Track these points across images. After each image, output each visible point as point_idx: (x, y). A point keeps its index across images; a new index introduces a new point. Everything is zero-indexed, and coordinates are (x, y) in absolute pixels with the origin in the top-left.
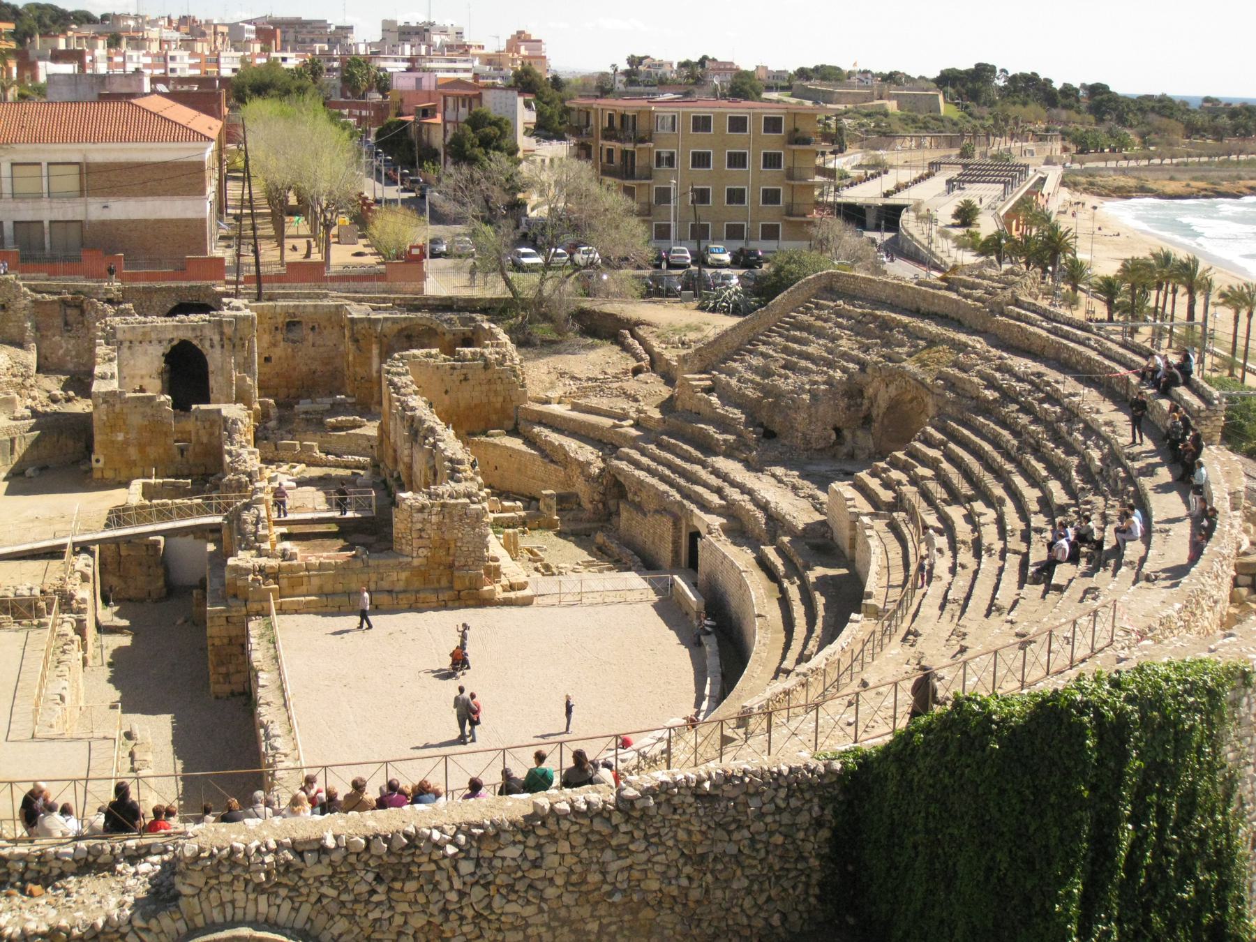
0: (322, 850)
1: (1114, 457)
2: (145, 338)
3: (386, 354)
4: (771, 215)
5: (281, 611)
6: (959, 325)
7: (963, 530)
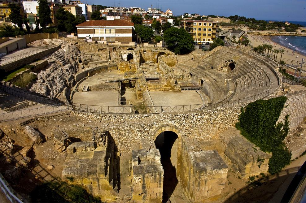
3: (158, 56)
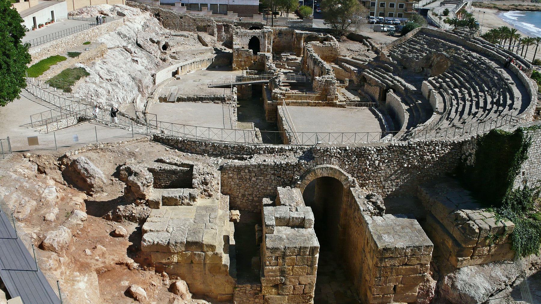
0: (346, 150)
1: (501, 79)
2: (245, 35)
4: (401, 11)
5: (288, 104)
6: (458, 44)
7: (459, 95)
